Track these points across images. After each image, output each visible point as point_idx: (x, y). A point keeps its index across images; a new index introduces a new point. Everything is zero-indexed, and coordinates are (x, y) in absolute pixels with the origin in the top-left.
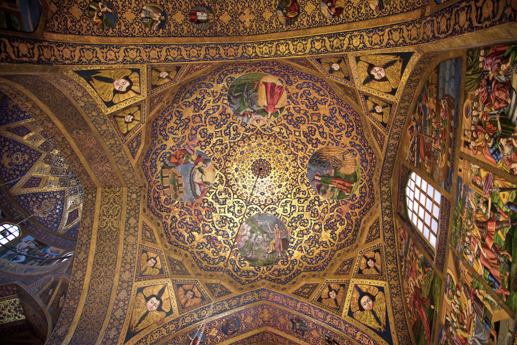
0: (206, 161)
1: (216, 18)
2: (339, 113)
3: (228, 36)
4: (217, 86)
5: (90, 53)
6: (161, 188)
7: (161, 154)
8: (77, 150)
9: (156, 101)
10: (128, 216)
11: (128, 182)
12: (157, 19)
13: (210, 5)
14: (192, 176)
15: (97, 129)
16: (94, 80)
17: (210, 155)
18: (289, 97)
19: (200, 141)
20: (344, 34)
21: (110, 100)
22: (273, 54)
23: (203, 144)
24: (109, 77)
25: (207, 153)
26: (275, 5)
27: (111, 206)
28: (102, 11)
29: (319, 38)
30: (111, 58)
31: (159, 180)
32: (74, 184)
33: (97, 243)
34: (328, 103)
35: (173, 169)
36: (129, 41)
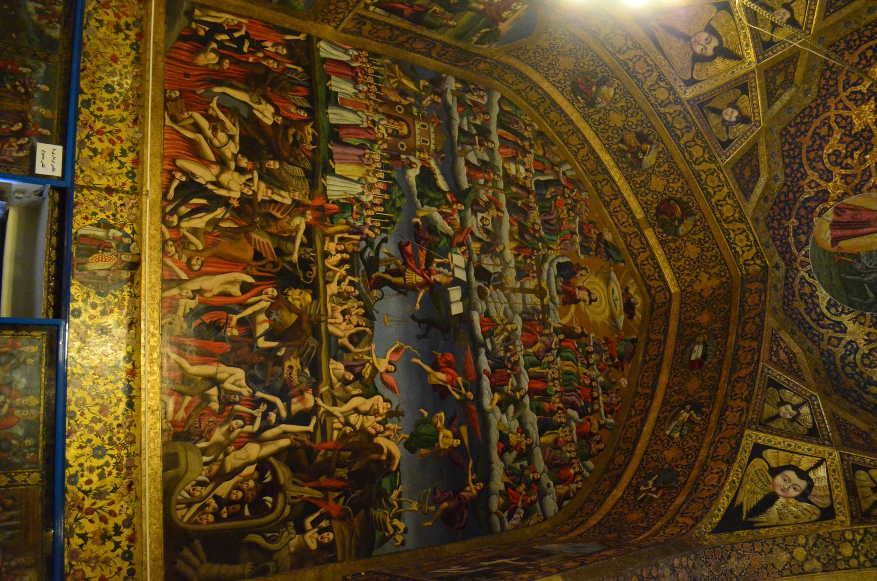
1: (703, 331)
2: (856, 84)
3: (729, 310)
4: (853, 333)
5: (694, 506)
9: (861, 441)
12: (688, 415)
13: (684, 342)
16: (756, 519)
18: (857, 190)
20: (662, 116)
21: (818, 512)
22: (743, 226)
24: (760, 497)
26: (675, 241)
28: (650, 487)
29: (686, 154)
30: (716, 479)
34: (846, 113)
36: (703, 453)
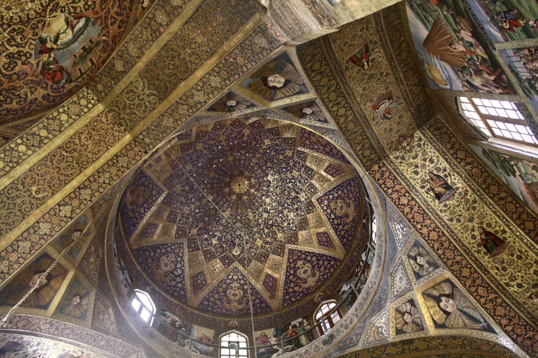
0: (43, 41)
6: (94, 67)
7: (54, 94)
8: (75, 183)
10: (120, 77)
11: (90, 106)
14: (68, 44)
15: (8, 172)
17: (34, 42)
19: (23, 63)
23: (23, 58)
25: (33, 47)
27: (132, 107)
31: (85, 76)
32: (303, 194)
33: (174, 89)
35: (69, 71)
